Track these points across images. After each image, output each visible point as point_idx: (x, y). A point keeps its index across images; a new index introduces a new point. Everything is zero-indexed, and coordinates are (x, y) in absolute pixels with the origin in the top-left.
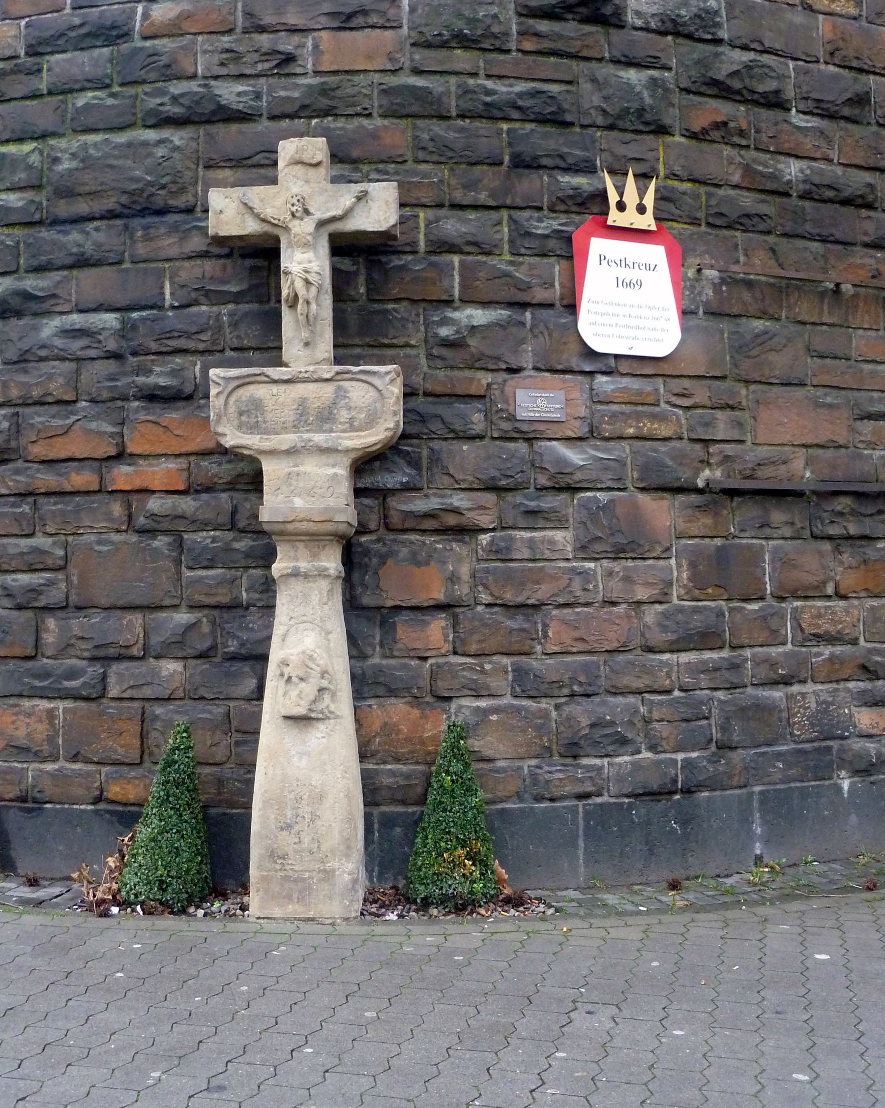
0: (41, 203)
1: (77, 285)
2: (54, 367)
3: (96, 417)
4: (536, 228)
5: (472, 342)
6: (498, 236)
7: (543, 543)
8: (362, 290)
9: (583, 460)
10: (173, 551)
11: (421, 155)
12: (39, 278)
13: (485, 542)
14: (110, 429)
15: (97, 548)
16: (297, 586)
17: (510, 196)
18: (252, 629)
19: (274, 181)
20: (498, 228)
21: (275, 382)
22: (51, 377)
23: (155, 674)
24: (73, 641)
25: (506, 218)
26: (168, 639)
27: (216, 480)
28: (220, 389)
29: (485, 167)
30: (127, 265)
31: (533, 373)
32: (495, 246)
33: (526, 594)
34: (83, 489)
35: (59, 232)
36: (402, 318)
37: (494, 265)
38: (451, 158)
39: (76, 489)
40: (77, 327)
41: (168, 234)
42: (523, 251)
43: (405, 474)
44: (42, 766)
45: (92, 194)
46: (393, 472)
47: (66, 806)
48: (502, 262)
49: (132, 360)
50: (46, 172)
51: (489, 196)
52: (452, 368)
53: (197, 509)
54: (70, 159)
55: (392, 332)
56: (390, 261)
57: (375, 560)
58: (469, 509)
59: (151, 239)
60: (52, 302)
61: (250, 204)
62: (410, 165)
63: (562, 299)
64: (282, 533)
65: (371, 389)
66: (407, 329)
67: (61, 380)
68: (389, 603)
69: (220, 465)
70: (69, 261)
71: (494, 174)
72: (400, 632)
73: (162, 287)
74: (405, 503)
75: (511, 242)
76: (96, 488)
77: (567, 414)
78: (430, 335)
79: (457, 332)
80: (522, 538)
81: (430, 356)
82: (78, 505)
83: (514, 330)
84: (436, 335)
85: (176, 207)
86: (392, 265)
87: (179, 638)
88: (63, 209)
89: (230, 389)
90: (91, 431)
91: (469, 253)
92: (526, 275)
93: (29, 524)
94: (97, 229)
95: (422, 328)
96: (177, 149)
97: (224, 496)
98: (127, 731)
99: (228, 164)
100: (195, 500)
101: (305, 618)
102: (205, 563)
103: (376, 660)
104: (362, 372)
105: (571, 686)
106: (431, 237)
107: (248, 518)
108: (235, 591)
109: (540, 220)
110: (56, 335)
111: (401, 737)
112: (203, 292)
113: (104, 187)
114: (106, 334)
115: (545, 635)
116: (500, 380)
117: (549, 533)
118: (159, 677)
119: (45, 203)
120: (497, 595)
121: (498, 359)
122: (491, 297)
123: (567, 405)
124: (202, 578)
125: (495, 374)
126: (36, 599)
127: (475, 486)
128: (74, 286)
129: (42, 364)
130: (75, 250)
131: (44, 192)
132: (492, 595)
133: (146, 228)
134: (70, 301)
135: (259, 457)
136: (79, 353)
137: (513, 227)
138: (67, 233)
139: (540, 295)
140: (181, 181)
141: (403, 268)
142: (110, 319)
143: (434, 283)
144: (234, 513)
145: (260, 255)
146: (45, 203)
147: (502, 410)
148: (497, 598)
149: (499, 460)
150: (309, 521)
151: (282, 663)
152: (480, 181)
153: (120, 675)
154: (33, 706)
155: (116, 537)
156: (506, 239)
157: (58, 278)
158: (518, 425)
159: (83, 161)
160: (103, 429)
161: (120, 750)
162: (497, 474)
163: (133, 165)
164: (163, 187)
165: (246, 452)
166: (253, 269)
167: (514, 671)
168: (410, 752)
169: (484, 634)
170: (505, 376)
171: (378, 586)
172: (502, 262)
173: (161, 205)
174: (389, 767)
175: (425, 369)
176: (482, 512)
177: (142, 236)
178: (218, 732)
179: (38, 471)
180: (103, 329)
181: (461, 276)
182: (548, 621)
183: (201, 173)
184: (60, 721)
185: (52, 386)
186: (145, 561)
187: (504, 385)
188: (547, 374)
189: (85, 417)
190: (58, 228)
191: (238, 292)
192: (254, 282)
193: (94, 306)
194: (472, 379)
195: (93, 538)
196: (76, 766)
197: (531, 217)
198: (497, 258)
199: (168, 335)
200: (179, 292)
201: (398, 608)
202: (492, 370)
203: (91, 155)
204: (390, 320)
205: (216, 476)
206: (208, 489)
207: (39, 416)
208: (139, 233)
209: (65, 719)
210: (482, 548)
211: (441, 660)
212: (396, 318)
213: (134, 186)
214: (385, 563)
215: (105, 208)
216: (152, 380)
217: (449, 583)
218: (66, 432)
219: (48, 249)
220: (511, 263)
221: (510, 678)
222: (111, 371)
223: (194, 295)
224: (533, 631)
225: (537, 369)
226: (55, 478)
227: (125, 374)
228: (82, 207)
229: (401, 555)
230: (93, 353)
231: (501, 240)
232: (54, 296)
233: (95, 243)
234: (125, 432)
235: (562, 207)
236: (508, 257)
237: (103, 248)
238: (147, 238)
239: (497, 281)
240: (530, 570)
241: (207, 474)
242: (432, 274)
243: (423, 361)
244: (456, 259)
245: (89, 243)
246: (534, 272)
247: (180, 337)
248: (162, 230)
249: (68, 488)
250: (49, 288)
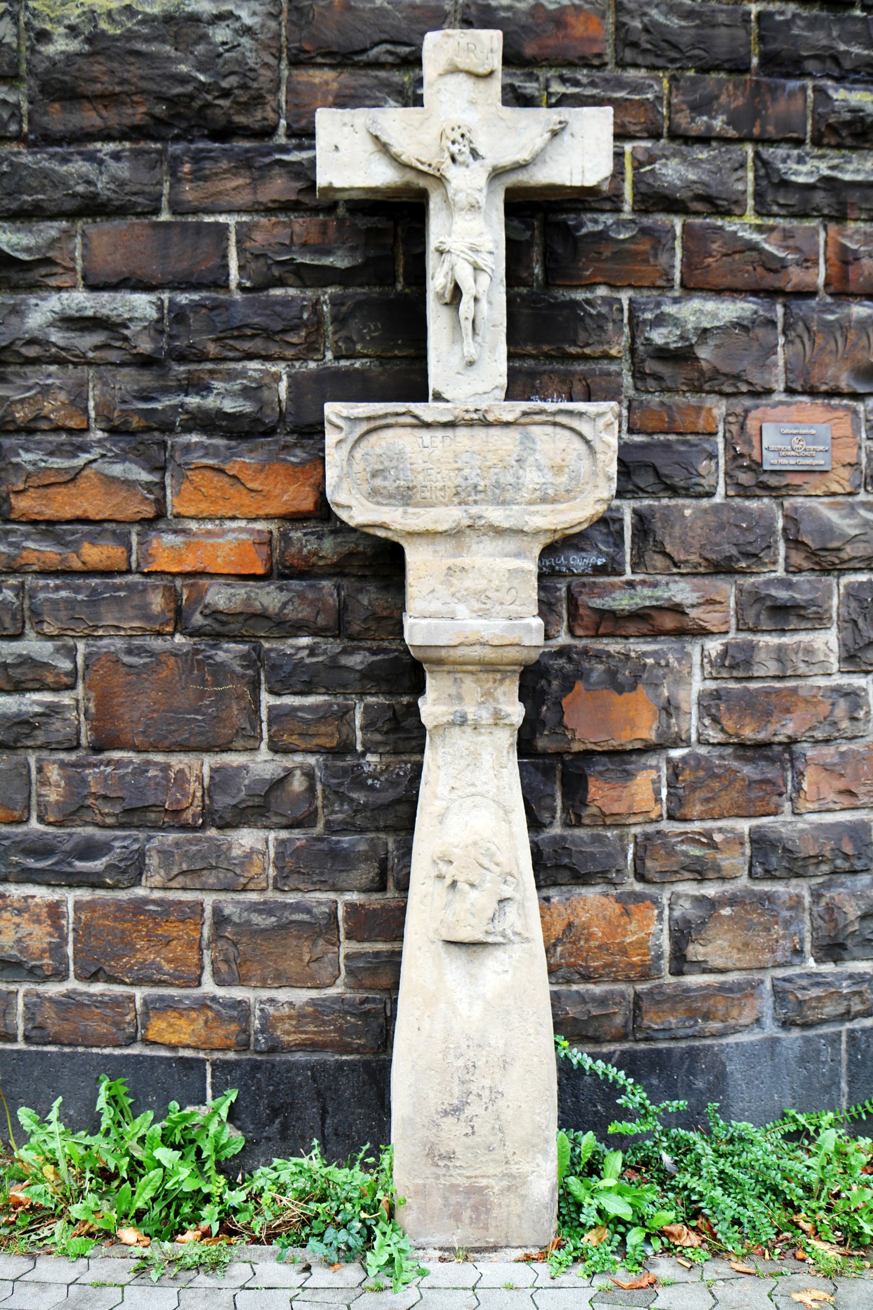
0: (17, 106)
1: (85, 246)
2: (49, 376)
3: (121, 458)
4: (796, 173)
5: (703, 353)
6: (740, 187)
7: (797, 653)
8: (537, 270)
9: (856, 526)
10: (247, 667)
11: (629, 55)
12: (18, 230)
13: (714, 654)
14: (145, 476)
15: (127, 659)
16: (461, 739)
17: (758, 123)
18: (372, 788)
19: (418, 101)
20: (740, 173)
21: (427, 425)
22: (46, 390)
23: (220, 851)
24: (90, 801)
25: (751, 154)
26: (243, 801)
27: (314, 559)
28: (342, 436)
29: (723, 75)
30: (165, 217)
31: (783, 397)
32: (736, 202)
33: (771, 728)
34: (101, 567)
35: (52, 156)
36: (600, 315)
37: (735, 233)
38: (673, 61)
39: (90, 567)
40: (90, 313)
41: (234, 172)
42: (775, 209)
43: (601, 553)
44: (41, 988)
45: (108, 99)
46: (583, 550)
47: (80, 1049)
48: (743, 226)
49: (181, 369)
50: (25, 53)
51: (728, 123)
52: (669, 390)
53: (284, 605)
54: (67, 36)
55: (582, 336)
56: (581, 225)
57: (555, 683)
58: (693, 606)
59: (206, 179)
60: (43, 271)
61: (384, 138)
62: (611, 71)
63: (827, 284)
64: (440, 662)
65: (576, 440)
66: (604, 331)
67: (62, 396)
68: (576, 747)
69: (320, 537)
70: (70, 205)
71: (736, 87)
72: (592, 789)
73: (225, 256)
74: (600, 596)
75: (758, 195)
76: (124, 567)
77: (833, 459)
78: (639, 341)
79: (682, 338)
80: (767, 646)
81: (639, 374)
82: (94, 591)
83: (760, 332)
84: (648, 341)
85: (246, 128)
86: (584, 231)
87: (257, 801)
88: (58, 118)
89: (356, 435)
90: (113, 480)
91: (697, 214)
92: (780, 247)
93: (14, 618)
94: (116, 156)
95: (626, 330)
96: (248, 30)
97: (327, 584)
98: (178, 938)
99: (328, 61)
100: (281, 589)
101: (473, 790)
102: (299, 687)
103: (556, 830)
104: (561, 412)
105: (833, 861)
106: (643, 188)
107: (365, 620)
108: (345, 730)
109: (800, 160)
110: (51, 325)
111: (593, 943)
112: (290, 268)
113: (126, 88)
114: (135, 327)
115: (798, 789)
116: (739, 410)
117: (803, 637)
118: (228, 859)
119: (25, 106)
120: (731, 731)
121: (737, 378)
122: (727, 281)
123: (833, 445)
124: (295, 709)
125: (733, 401)
126: (28, 736)
127: (702, 570)
128: (79, 246)
129: (28, 369)
130: (80, 189)
131: (24, 88)
132: (723, 730)
133: (197, 158)
134: (73, 270)
135: (402, 542)
136: (91, 355)
137: (762, 172)
138: (65, 160)
139: (796, 277)
140: (255, 85)
141: (602, 236)
143: (647, 261)
144: (342, 609)
145: (397, 219)
146: (25, 106)
147: (742, 455)
148: (731, 736)
149: (737, 532)
150: (483, 644)
151: (441, 859)
152: (717, 97)
153: (165, 854)
154: (26, 898)
155: (157, 644)
156: (750, 189)
157: (54, 233)
158: (764, 478)
159: (89, 40)
160: (132, 477)
161: (166, 967)
162: (734, 551)
163: (173, 53)
164: (226, 93)
165: (381, 533)
166: (372, 233)
167: (752, 841)
168: (605, 966)
169: (713, 790)
170: (748, 402)
171: (560, 723)
172: (743, 226)
173: (218, 120)
174: (575, 987)
175: (631, 392)
176: (711, 608)
177: (191, 173)
178: (321, 942)
179: (27, 536)
180: (131, 320)
181: (684, 248)
183: (286, 73)
184: (69, 922)
185: (48, 406)
186: (203, 682)
187: (745, 418)
188: (805, 399)
189: (103, 456)
190: (51, 150)
191: (347, 269)
192: (372, 253)
193: (115, 280)
194: (699, 409)
195: (120, 644)
196: (98, 988)
197: (789, 156)
198: (736, 220)
199: (236, 333)
200: (253, 265)
201: (588, 754)
202: (727, 395)
203: (103, 32)
204: (582, 319)
205: (315, 554)
206: (301, 574)
207: (27, 450)
208: (187, 168)
209: (77, 920)
210: (710, 661)
211: (650, 829)
212: (591, 315)
214: (571, 689)
215: (127, 121)
216: (211, 402)
217: (664, 715)
218: (73, 480)
219: (35, 184)
220: (759, 229)
221: (748, 851)
222: (143, 384)
223: (276, 272)
224: (781, 783)
225: (790, 391)
226: (56, 549)
227: (166, 390)
228: (89, 118)
229: (594, 677)
230: (113, 356)
231: (745, 192)
232: (47, 262)
233: (113, 179)
234: (168, 481)
235: (833, 141)
236: (751, 218)
237: (127, 189)
238: (198, 176)
239: (737, 257)
240: (777, 692)
241: (300, 551)
242: (645, 246)
243: (627, 380)
244: (678, 223)
245: (105, 178)
246: (791, 242)
247: (253, 336)
248: (224, 164)
249: (77, 565)
250: (39, 249)
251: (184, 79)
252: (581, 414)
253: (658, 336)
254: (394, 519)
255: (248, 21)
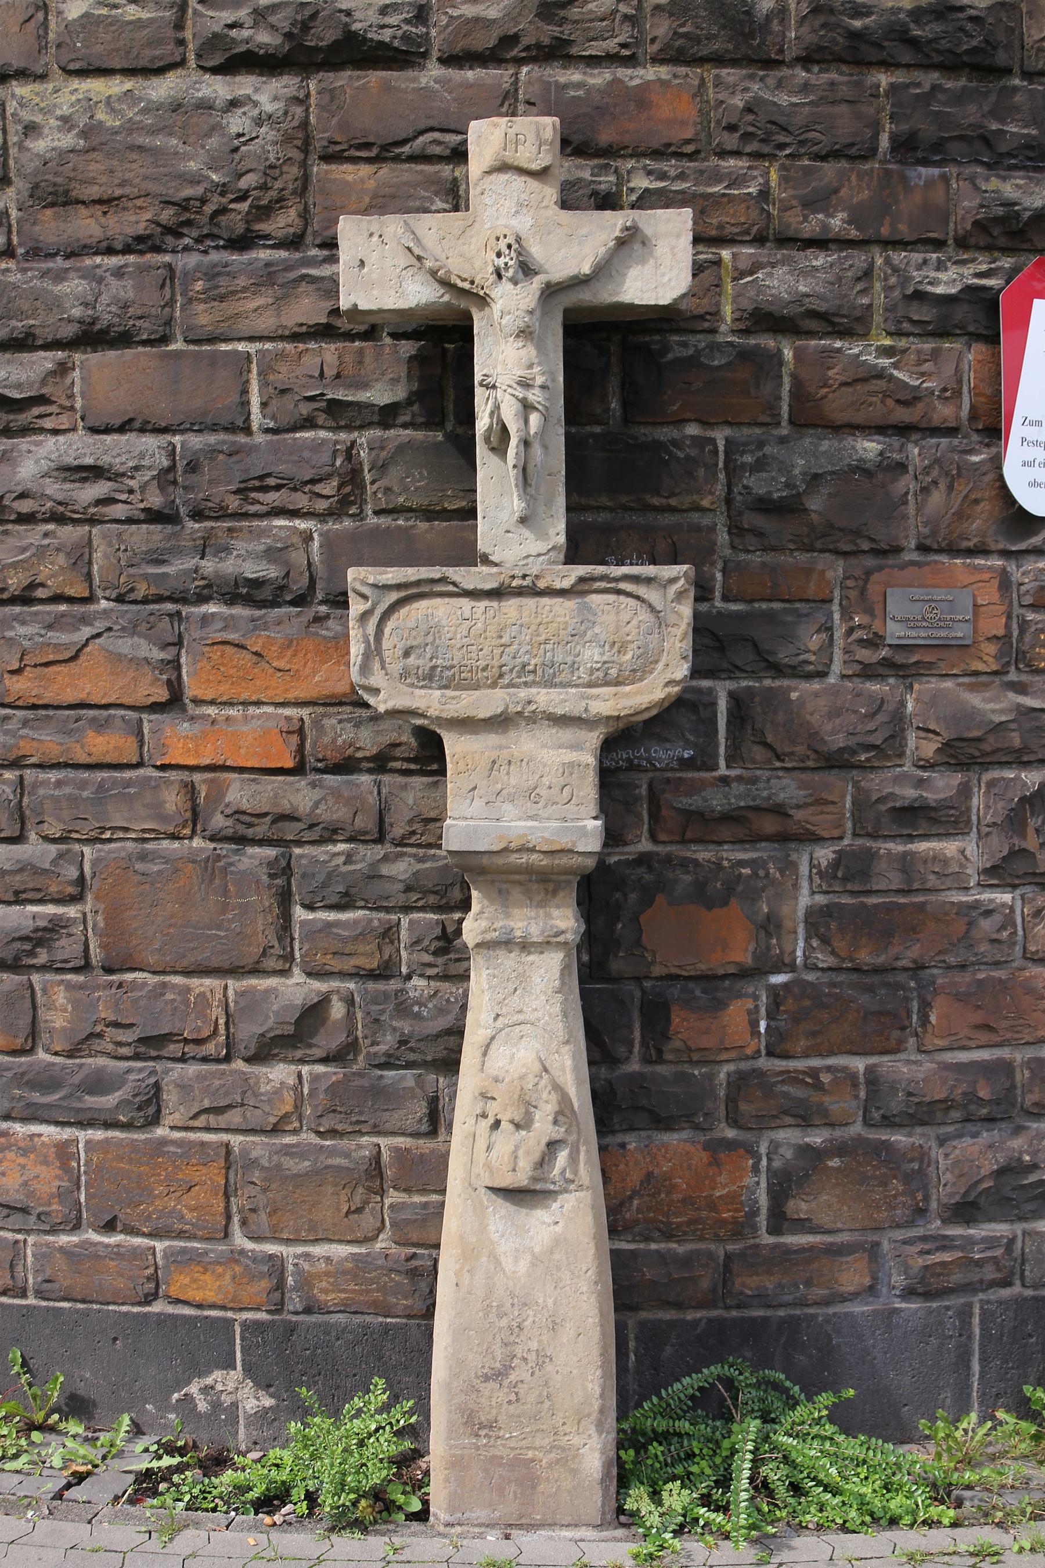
2: (46, 535)
5: (815, 504)
8: (614, 404)
13: (824, 863)
17: (887, 221)
18: (418, 1016)
23: (247, 1085)
26: (271, 1029)
29: (844, 164)
31: (915, 556)
32: (858, 319)
35: (44, 274)
36: (688, 458)
43: (688, 744)
46: (667, 740)
53: (317, 804)
54: (59, 129)
56: (666, 349)
57: (633, 897)
58: (798, 807)
59: (222, 298)
60: (36, 411)
68: (657, 971)
70: (68, 331)
71: (860, 176)
72: (675, 1020)
73: (245, 392)
74: (688, 794)
76: (135, 760)
79: (787, 485)
81: (736, 530)
90: (119, 657)
91: (811, 334)
94: (119, 273)
95: (722, 476)
97: (365, 779)
100: (313, 785)
102: (334, 899)
103: (634, 1066)
104: (626, 578)
105: (965, 1106)
107: (410, 822)
109: (940, 266)
111: (676, 1197)
113: (127, 190)
115: (924, 1020)
120: (843, 954)
121: (857, 533)
124: (329, 925)
125: (852, 561)
127: (811, 764)
132: (833, 953)
134: (72, 408)
138: (60, 276)
141: (693, 363)
142: (150, 447)
152: (836, 191)
153: (184, 1088)
159: (84, 134)
168: (690, 1222)
170: (870, 562)
171: (638, 943)
174: (653, 1246)
175: (728, 552)
176: (819, 808)
182: (929, 998)
187: (866, 581)
189: (110, 629)
193: (117, 422)
194: (808, 571)
197: (925, 262)
199: (257, 483)
202: (845, 554)
207: (23, 623)
211: (744, 1066)
212: (678, 459)
213: (188, 192)
214: (651, 903)
217: (763, 934)
220: (887, 352)
221: (863, 1094)
224: (903, 1014)
226: (58, 738)
228: (87, 225)
235: (983, 241)
240: (901, 907)
241: (334, 741)
243: (723, 537)
247: (278, 488)
251: (194, 180)
252: (649, 581)
253: (758, 484)
254: (432, 702)
255: (269, 107)
